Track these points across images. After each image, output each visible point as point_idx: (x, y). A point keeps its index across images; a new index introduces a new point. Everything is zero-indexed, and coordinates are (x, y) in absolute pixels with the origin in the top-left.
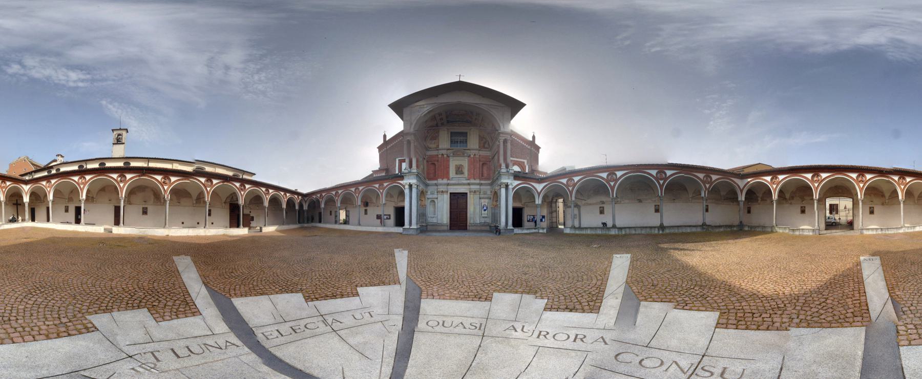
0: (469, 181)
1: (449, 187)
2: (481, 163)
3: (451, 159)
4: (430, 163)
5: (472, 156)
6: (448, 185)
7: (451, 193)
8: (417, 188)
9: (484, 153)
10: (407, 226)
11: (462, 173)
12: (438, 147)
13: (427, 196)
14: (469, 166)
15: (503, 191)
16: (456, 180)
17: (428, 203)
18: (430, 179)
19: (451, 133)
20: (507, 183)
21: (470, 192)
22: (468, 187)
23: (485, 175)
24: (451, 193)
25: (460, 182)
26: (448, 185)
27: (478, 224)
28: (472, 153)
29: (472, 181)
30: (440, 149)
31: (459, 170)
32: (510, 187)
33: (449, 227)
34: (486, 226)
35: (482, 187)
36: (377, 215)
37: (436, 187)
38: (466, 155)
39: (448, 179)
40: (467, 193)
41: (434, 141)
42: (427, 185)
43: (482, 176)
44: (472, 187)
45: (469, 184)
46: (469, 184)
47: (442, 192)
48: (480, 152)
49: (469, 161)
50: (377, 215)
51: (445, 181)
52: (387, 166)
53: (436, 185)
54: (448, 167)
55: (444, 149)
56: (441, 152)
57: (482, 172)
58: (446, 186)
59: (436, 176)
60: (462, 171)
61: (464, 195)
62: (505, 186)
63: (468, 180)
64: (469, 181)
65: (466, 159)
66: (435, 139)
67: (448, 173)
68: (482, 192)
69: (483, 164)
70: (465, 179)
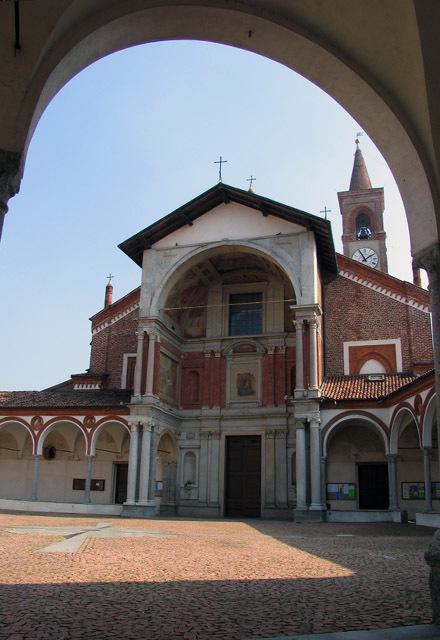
0: (263, 410)
1: (223, 423)
3: (229, 362)
4: (189, 370)
5: (271, 352)
6: (221, 418)
7: (227, 437)
8: (152, 432)
10: (130, 501)
11: (252, 393)
12: (204, 336)
13: (180, 443)
14: (264, 375)
16: (236, 408)
17: (181, 457)
18: (187, 407)
21: (266, 434)
24: (227, 437)
25: (246, 412)
26: (221, 418)
27: (283, 504)
28: (272, 343)
29: (271, 409)
30: (209, 341)
31: (245, 386)
32: (314, 426)
33: (222, 511)
36: (75, 480)
37: (198, 424)
39: (223, 406)
40: (260, 436)
41: (197, 320)
42: (180, 420)
44: (269, 422)
46: (264, 417)
47: (210, 434)
50: (75, 480)
51: (216, 411)
52: (106, 370)
53: (197, 419)
54: (222, 380)
55: (215, 341)
58: (217, 423)
60: (250, 387)
61: (255, 440)
62: (302, 426)
64: (263, 410)
66: (200, 315)
67: (222, 392)
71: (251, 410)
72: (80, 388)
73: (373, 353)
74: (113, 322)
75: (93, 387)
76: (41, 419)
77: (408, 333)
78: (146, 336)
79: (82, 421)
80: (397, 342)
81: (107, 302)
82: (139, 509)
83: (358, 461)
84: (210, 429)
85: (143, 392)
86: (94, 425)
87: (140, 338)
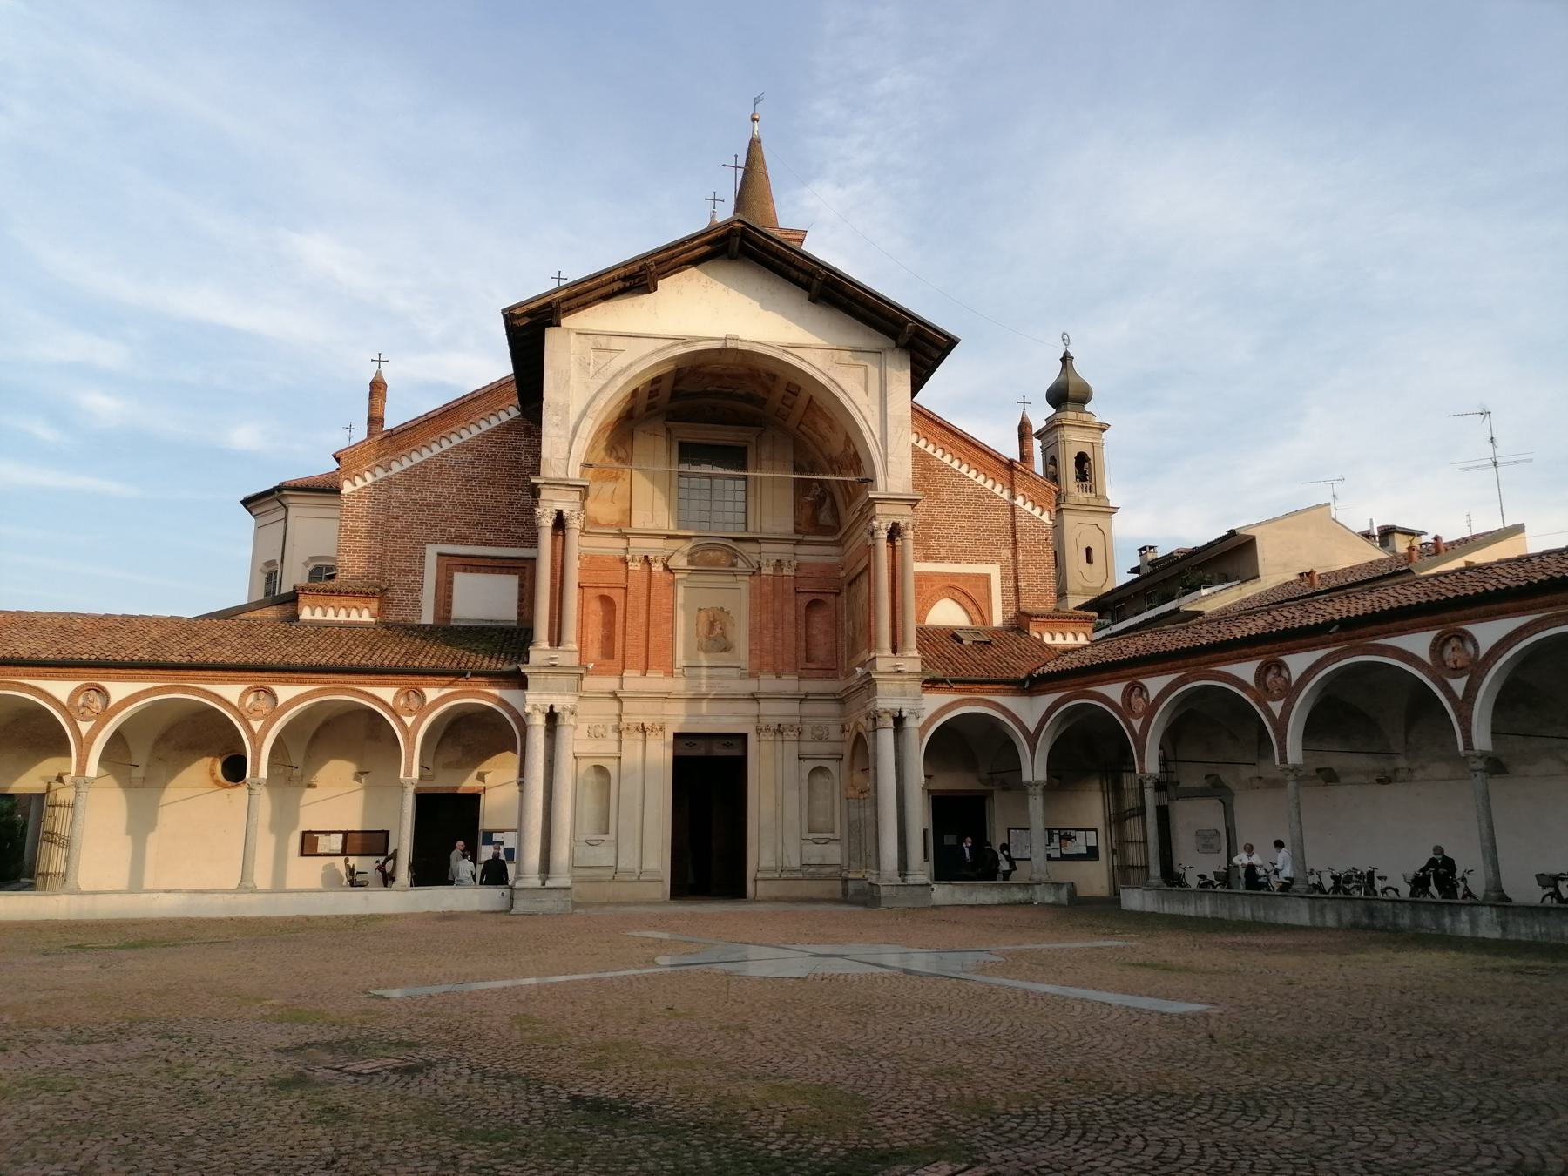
0: (751, 686)
2: (804, 600)
9: (816, 554)
14: (753, 611)
15: (886, 738)
19: (681, 444)
20: (900, 712)
21: (759, 732)
22: (751, 708)
23: (820, 653)
24: (676, 735)
27: (794, 870)
29: (768, 683)
32: (912, 724)
34: (828, 878)
35: (809, 708)
38: (741, 565)
39: (670, 673)
40: (744, 737)
43: (808, 660)
44: (767, 708)
45: (754, 698)
46: (754, 698)
48: (802, 549)
49: (757, 598)
56: (640, 546)
57: (807, 635)
59: (618, 653)
60: (724, 635)
63: (752, 675)
65: (744, 583)
68: (807, 729)
69: (813, 605)
70: (735, 672)
71: (725, 683)
72: (319, 615)
73: (956, 589)
74: (396, 468)
75: (354, 617)
76: (273, 695)
77: (1015, 555)
78: (560, 523)
79: (390, 701)
80: (994, 571)
81: (375, 421)
82: (555, 894)
83: (932, 787)
84: (640, 720)
85: (556, 639)
86: (423, 710)
87: (547, 523)
